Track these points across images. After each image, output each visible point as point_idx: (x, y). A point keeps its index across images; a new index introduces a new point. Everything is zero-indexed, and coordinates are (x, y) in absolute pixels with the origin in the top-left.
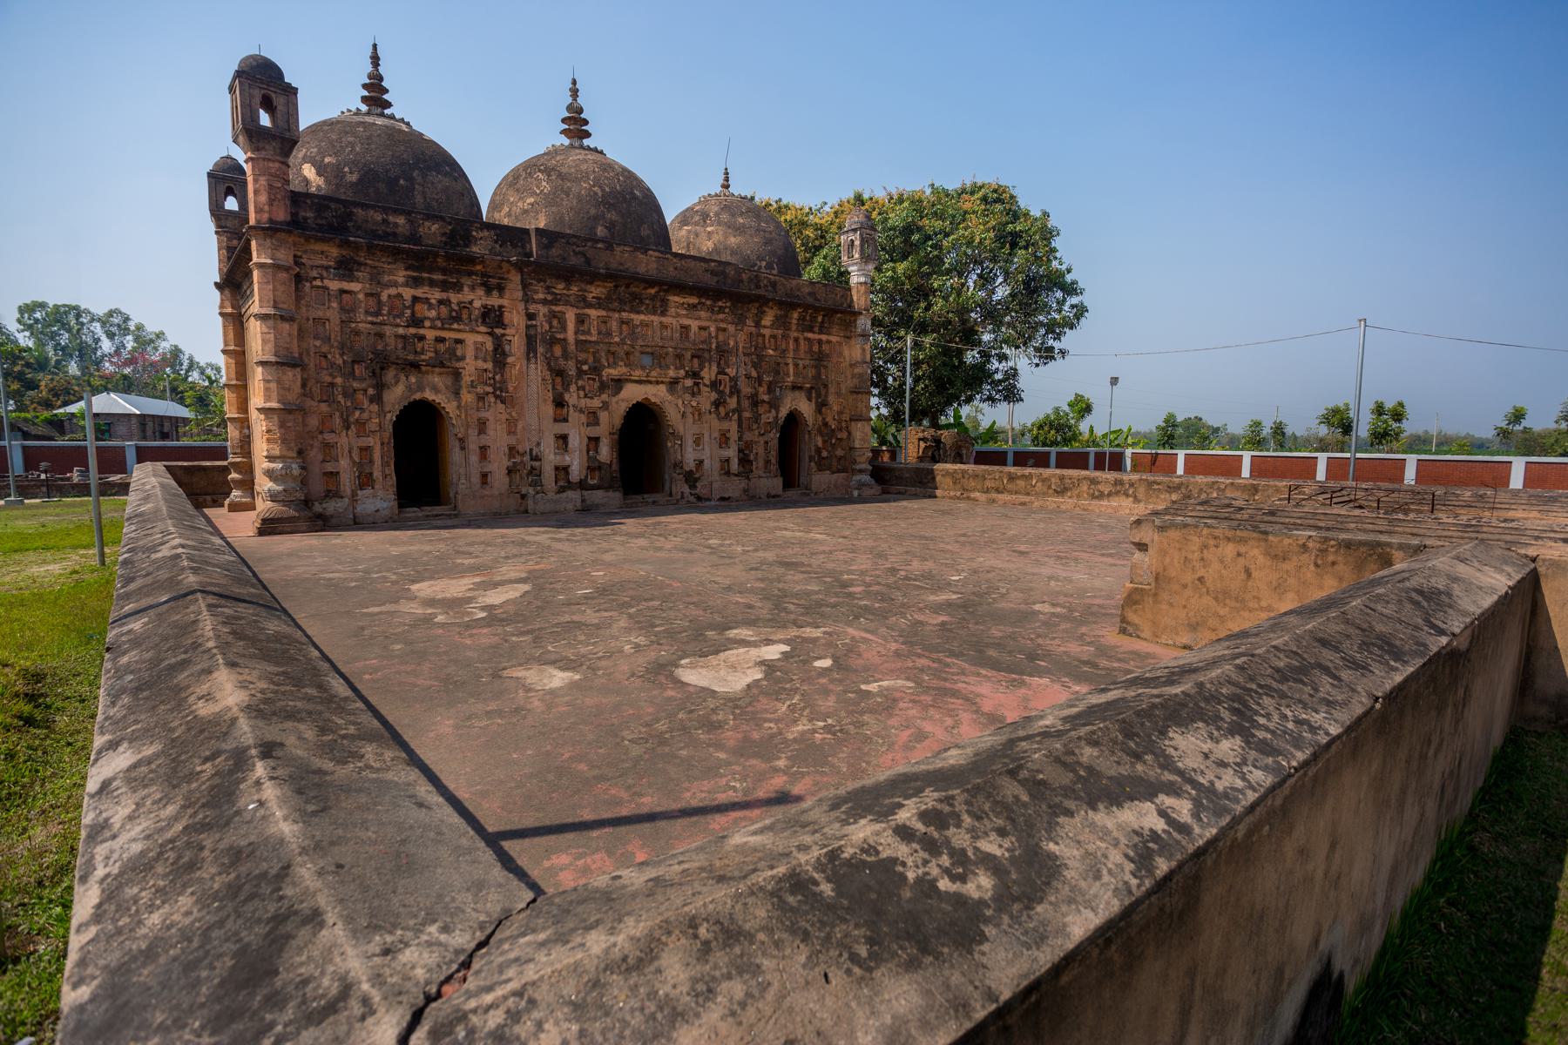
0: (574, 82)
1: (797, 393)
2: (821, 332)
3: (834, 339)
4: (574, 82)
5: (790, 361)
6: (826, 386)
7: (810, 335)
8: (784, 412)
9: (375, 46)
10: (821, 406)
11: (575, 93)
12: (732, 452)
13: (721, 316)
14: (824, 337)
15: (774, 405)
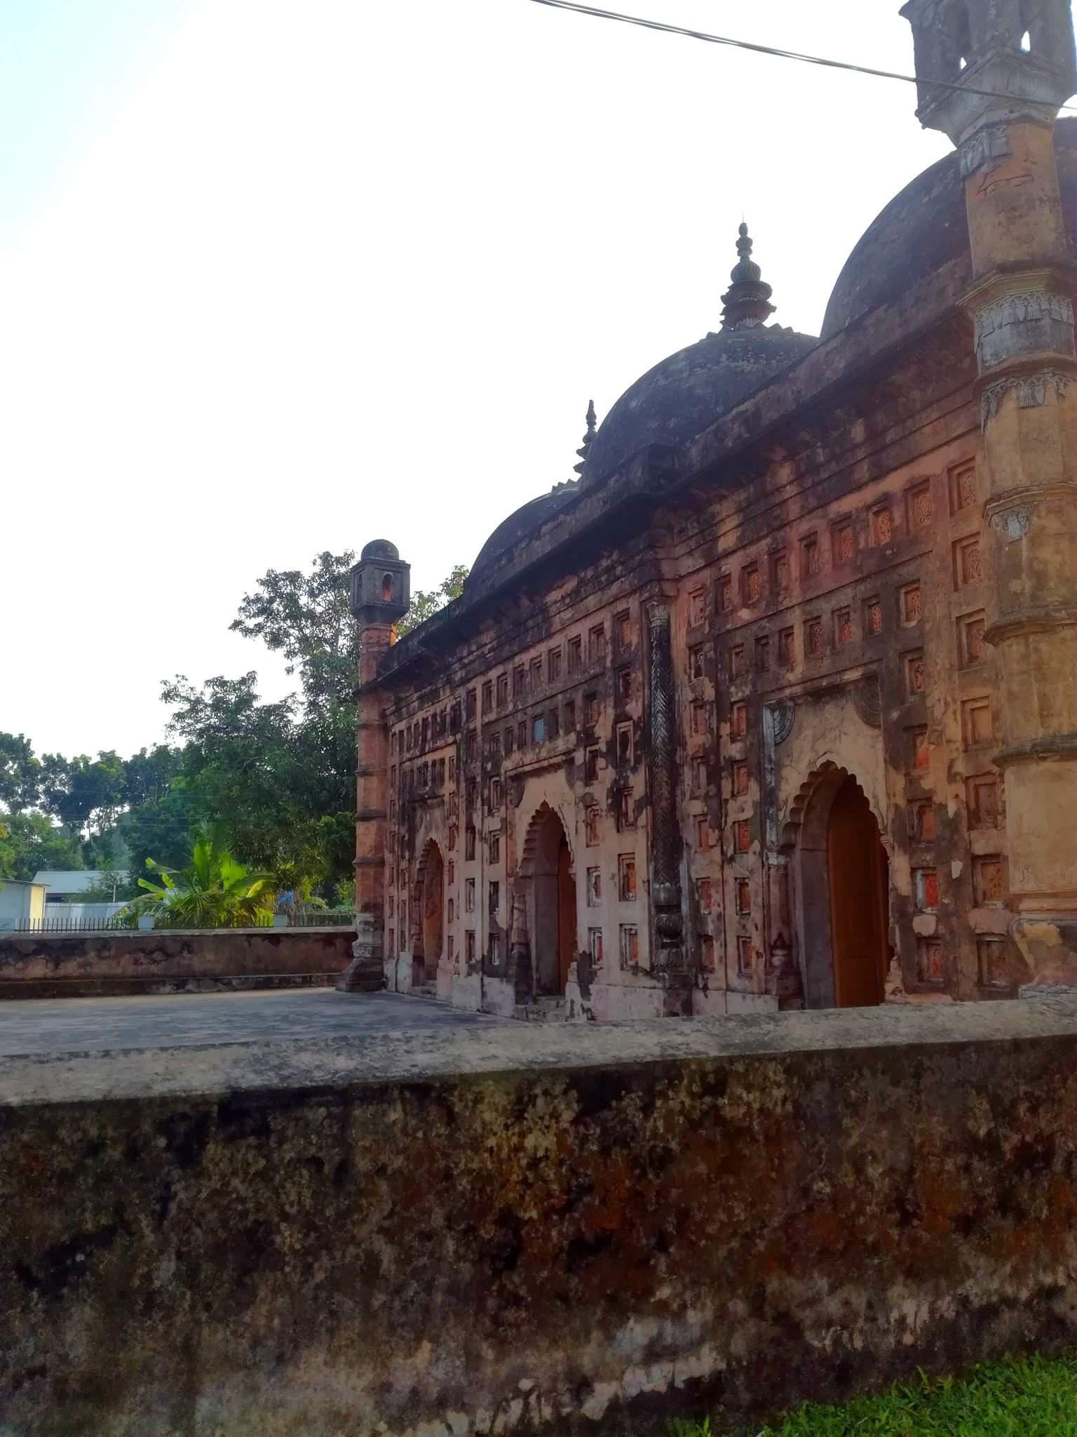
0: (743, 229)
1: (831, 711)
2: (880, 473)
3: (932, 465)
4: (743, 229)
5: (795, 619)
6: (916, 653)
7: (849, 503)
8: (792, 782)
9: (591, 403)
10: (905, 740)
11: (744, 245)
12: (638, 912)
13: (614, 589)
14: (894, 483)
15: (759, 765)
